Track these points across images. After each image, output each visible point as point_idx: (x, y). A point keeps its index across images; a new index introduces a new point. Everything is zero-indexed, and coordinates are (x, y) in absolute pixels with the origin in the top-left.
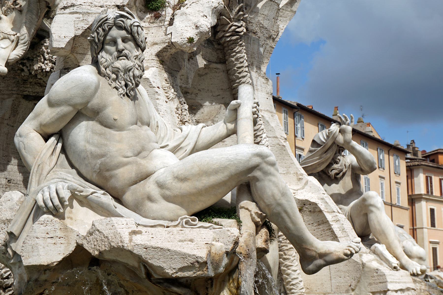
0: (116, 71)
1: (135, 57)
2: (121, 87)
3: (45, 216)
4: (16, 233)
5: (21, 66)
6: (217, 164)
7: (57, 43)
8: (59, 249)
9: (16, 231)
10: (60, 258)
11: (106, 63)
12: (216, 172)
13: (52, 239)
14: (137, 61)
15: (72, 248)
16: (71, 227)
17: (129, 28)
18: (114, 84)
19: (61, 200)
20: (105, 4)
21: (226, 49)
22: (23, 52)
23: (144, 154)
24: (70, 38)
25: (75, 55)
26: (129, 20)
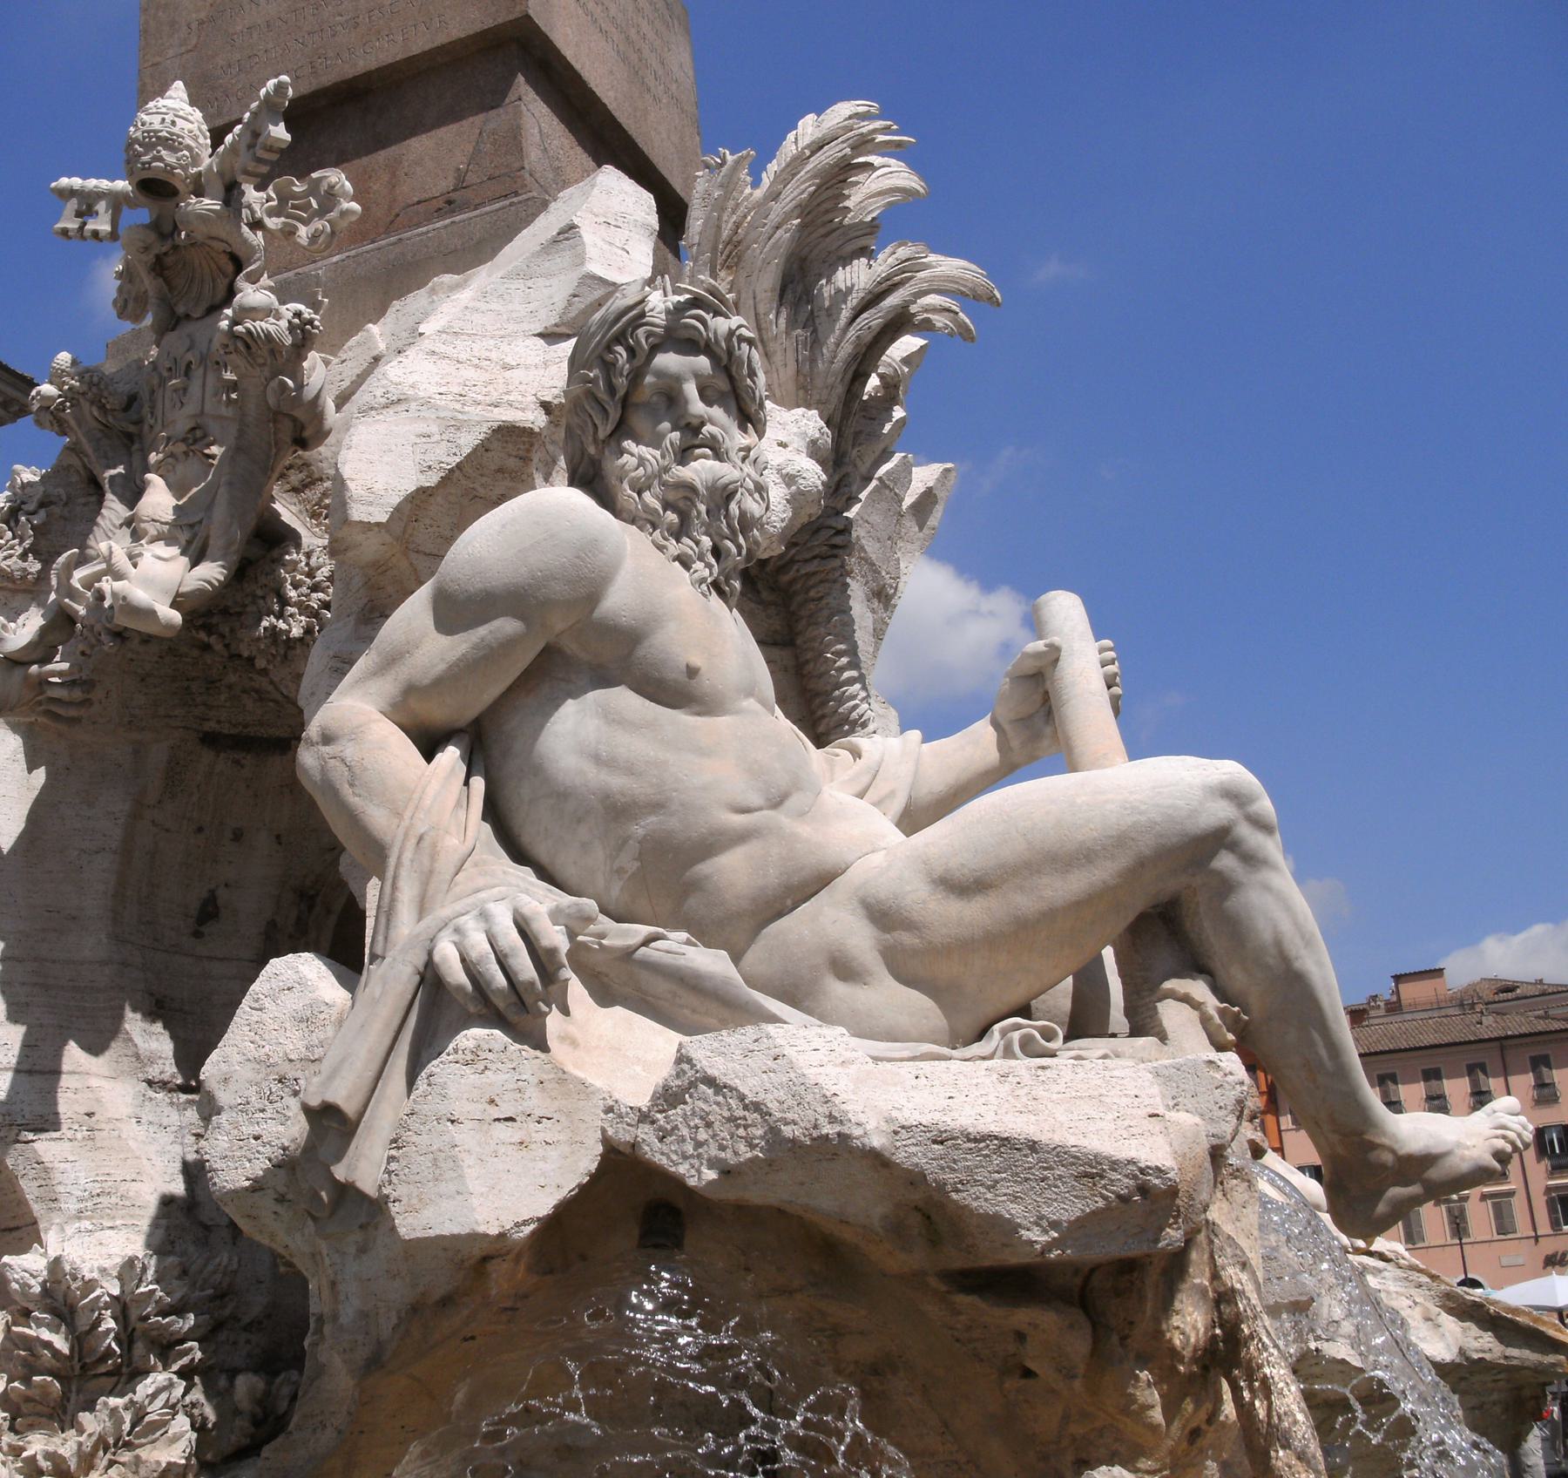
0: (682, 498)
1: (743, 453)
2: (701, 558)
3: (477, 1033)
4: (350, 1108)
5: (203, 636)
6: (1092, 826)
7: (363, 508)
8: (541, 1165)
9: (349, 1097)
10: (544, 1205)
11: (641, 471)
12: (1084, 856)
13: (510, 1124)
14: (748, 468)
15: (587, 1161)
16: (580, 1074)
17: (723, 344)
18: (673, 547)
19: (543, 959)
20: (506, 398)
21: (799, 599)
22: (222, 573)
23: (793, 802)
24: (401, 494)
25: (413, 556)
26: (720, 319)
